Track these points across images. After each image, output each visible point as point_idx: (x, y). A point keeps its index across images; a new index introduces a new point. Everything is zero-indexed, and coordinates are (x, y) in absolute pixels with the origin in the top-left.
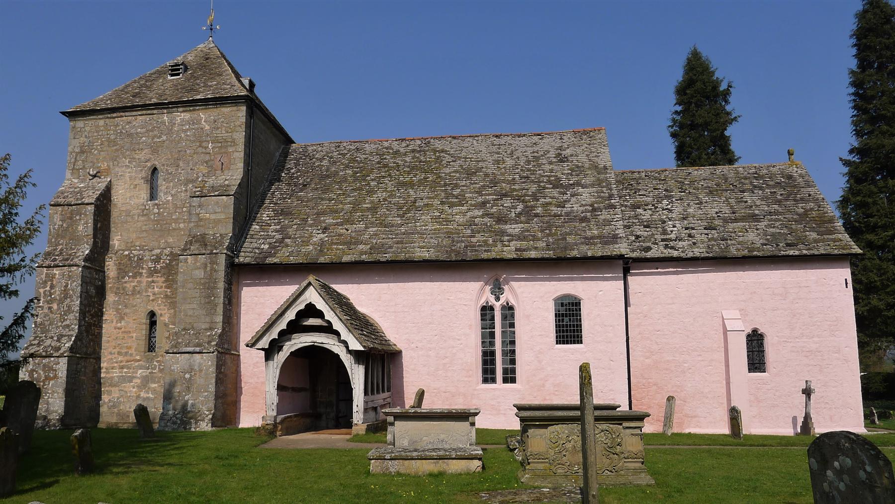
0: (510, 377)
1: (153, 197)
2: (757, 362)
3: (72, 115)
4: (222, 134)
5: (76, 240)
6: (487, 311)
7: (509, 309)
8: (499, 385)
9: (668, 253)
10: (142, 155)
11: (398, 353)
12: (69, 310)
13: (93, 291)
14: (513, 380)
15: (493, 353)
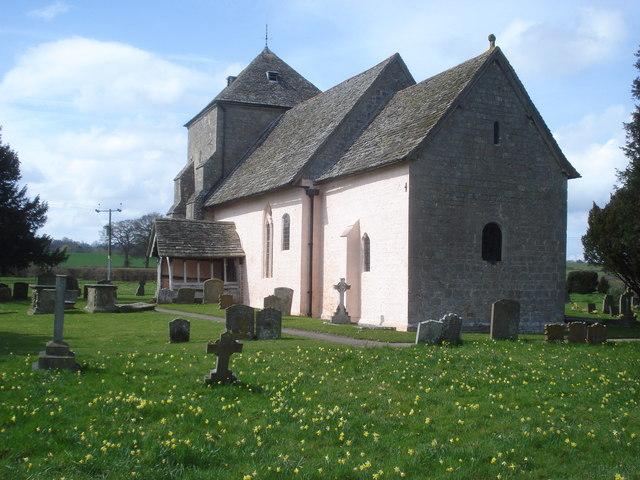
3: (188, 125)
8: (270, 279)
11: (242, 260)
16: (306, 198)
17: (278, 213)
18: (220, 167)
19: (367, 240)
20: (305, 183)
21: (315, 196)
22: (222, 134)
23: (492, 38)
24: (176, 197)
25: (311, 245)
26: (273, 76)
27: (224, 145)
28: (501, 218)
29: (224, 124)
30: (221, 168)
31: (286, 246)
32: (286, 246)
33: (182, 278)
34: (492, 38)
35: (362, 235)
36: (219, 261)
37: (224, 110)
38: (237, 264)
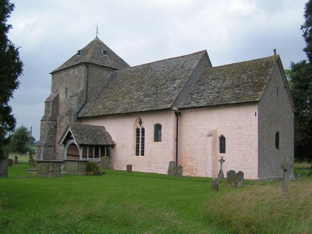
0: (143, 155)
1: (67, 96)
2: (223, 150)
3: (52, 73)
4: (79, 75)
5: (49, 112)
6: (138, 130)
7: (143, 130)
8: (140, 156)
9: (196, 105)
10: (64, 84)
11: (113, 146)
12: (46, 133)
13: (52, 127)
14: (144, 155)
15: (139, 146)
16: (174, 114)
17: (149, 125)
18: (85, 96)
19: (222, 139)
20: (175, 108)
21: (178, 114)
22: (86, 79)
23: (275, 51)
24: (47, 111)
25: (177, 140)
26: (105, 52)
27: (87, 86)
28: (280, 130)
29: (88, 76)
30: (85, 98)
31: (157, 138)
32: (157, 138)
33: (86, 157)
34: (275, 51)
35: (219, 135)
36: (103, 147)
37: (88, 68)
38: (110, 148)
